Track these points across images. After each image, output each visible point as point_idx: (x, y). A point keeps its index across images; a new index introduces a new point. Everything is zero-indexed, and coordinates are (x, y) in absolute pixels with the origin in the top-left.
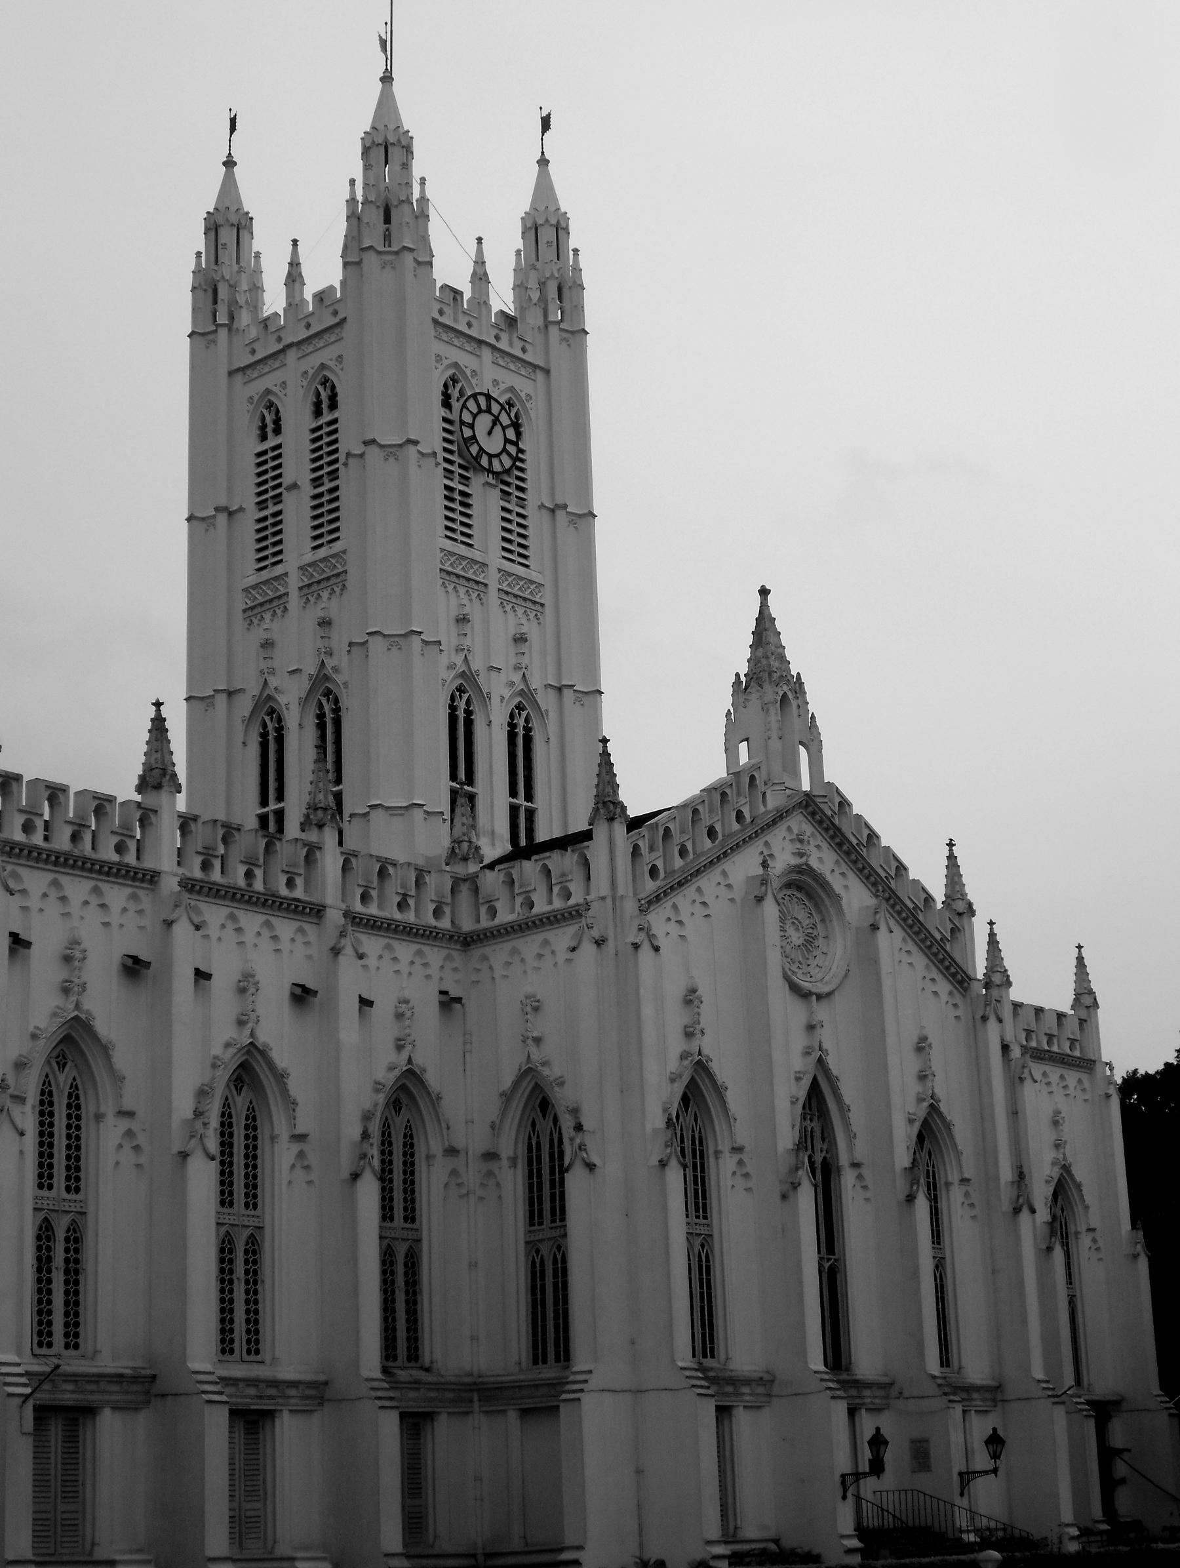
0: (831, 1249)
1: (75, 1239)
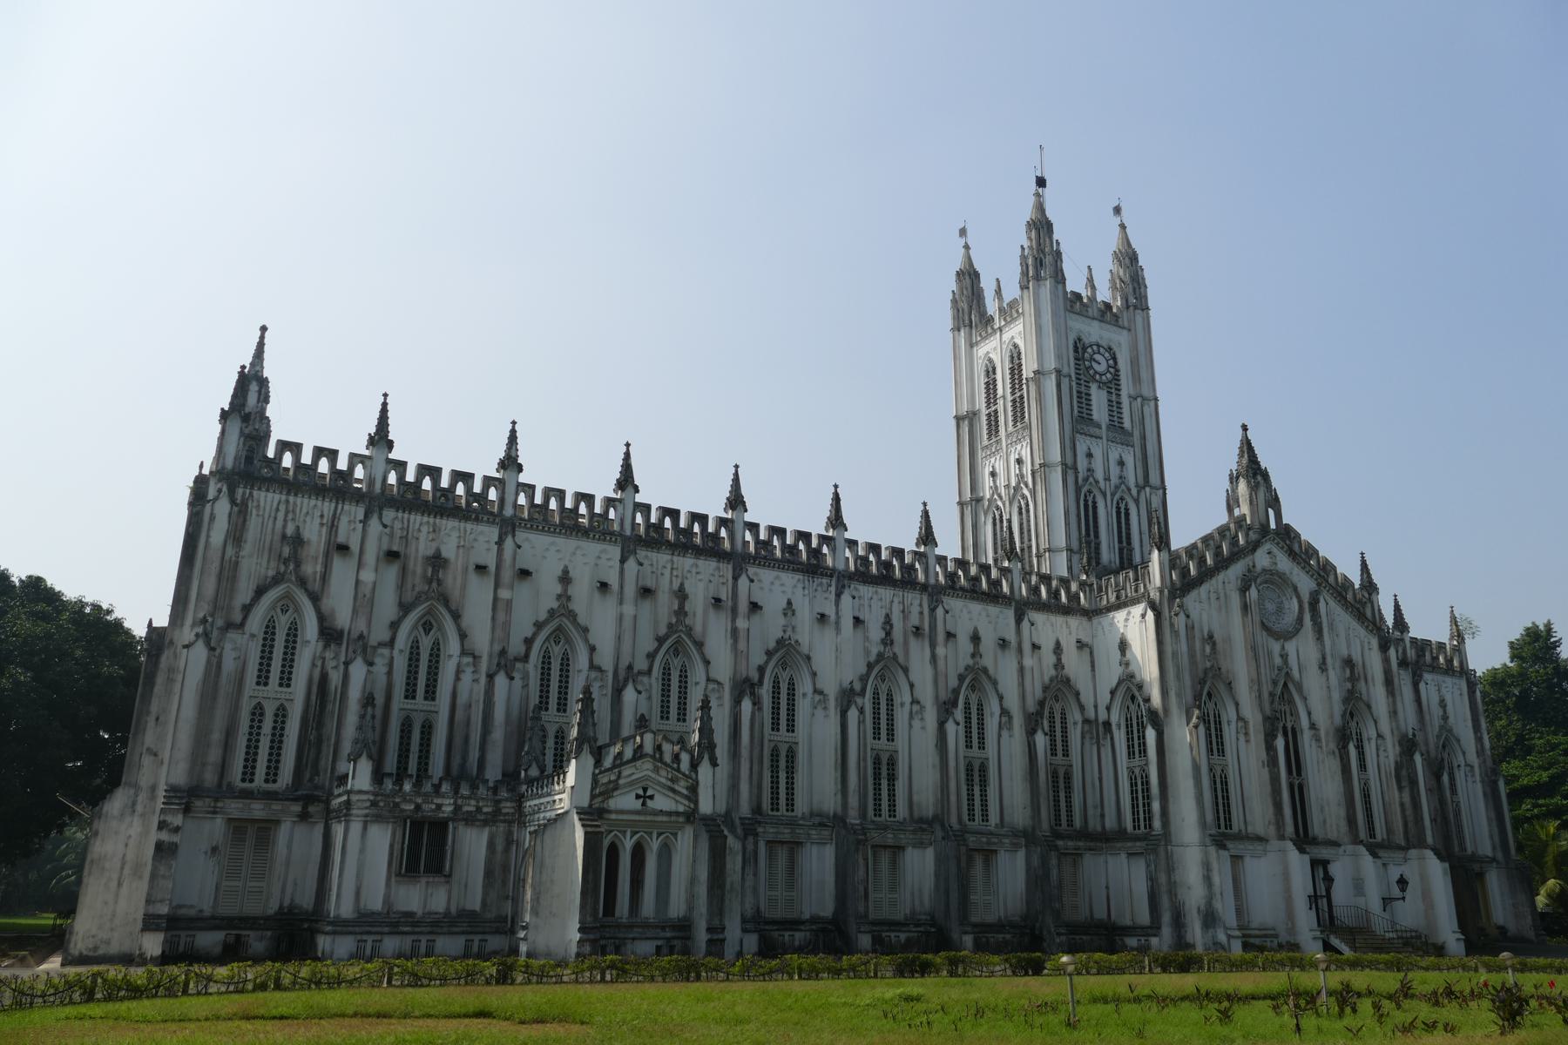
0: (1299, 774)
1: (892, 763)
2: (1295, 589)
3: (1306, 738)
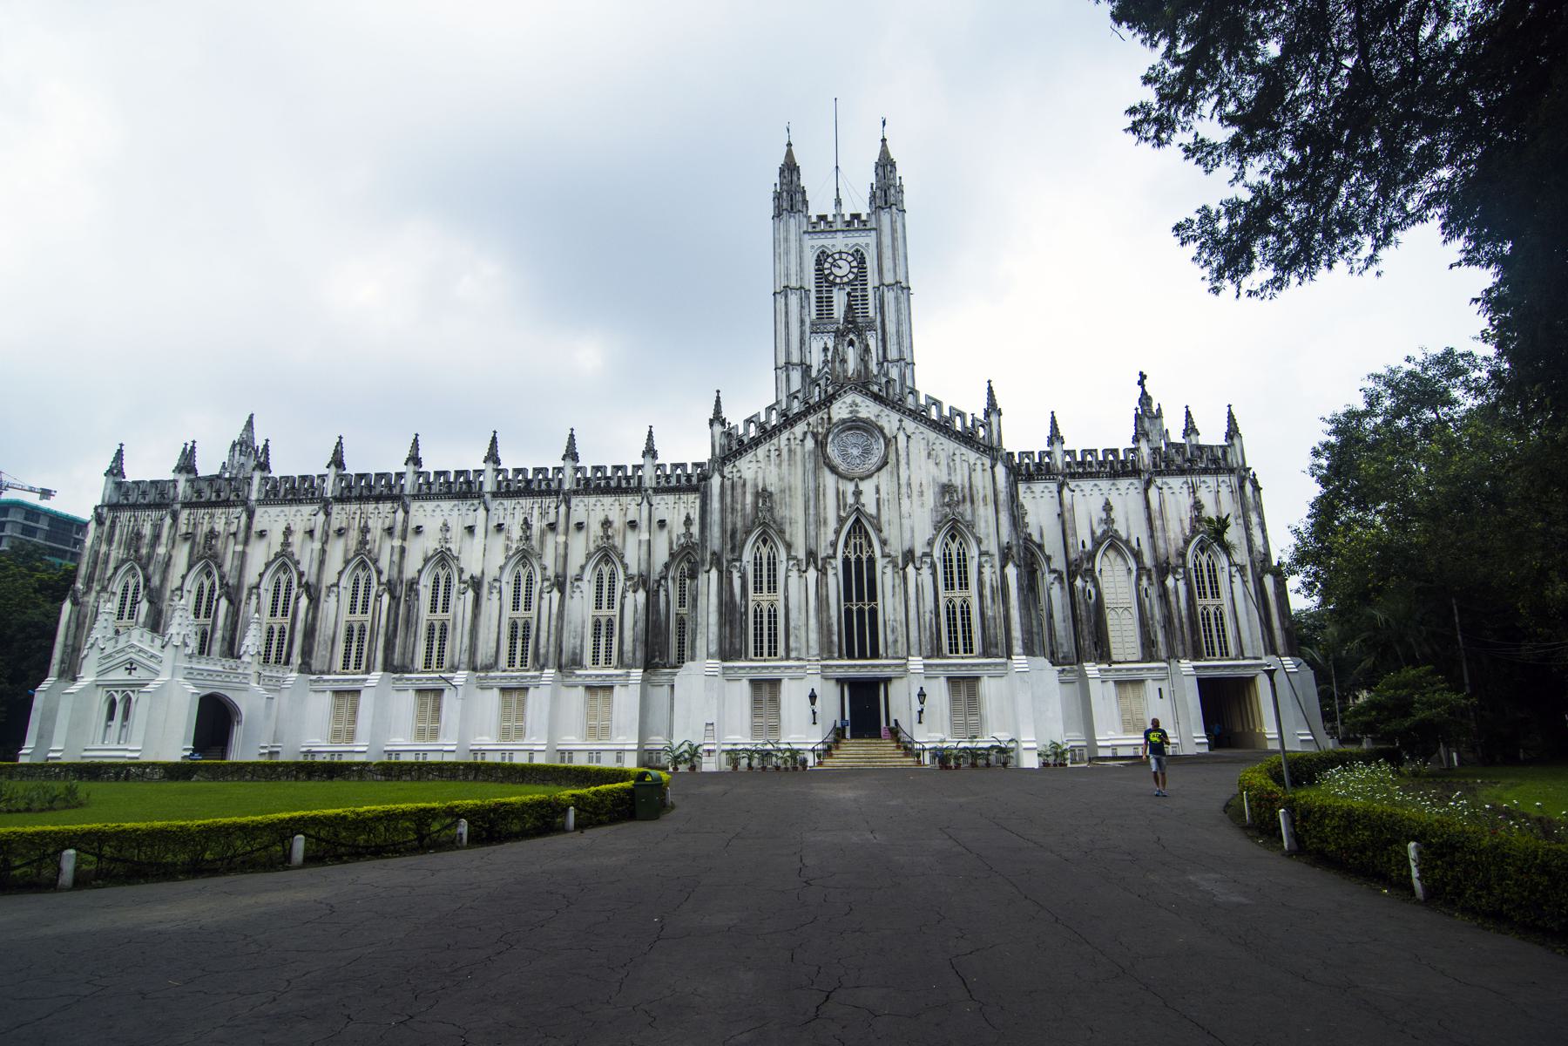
2: (881, 430)
3: (880, 563)
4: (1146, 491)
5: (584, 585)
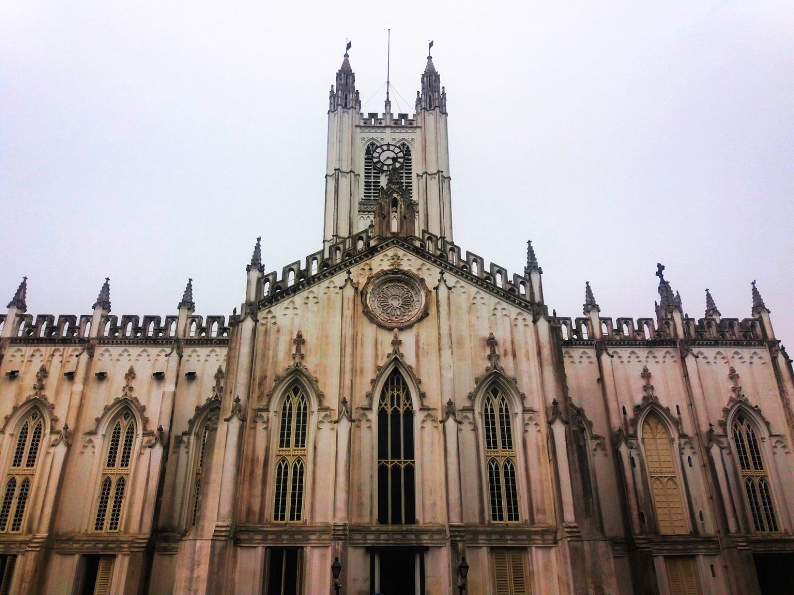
1: (26, 484)
2: (423, 280)
3: (418, 417)
4: (683, 359)
5: (98, 440)
